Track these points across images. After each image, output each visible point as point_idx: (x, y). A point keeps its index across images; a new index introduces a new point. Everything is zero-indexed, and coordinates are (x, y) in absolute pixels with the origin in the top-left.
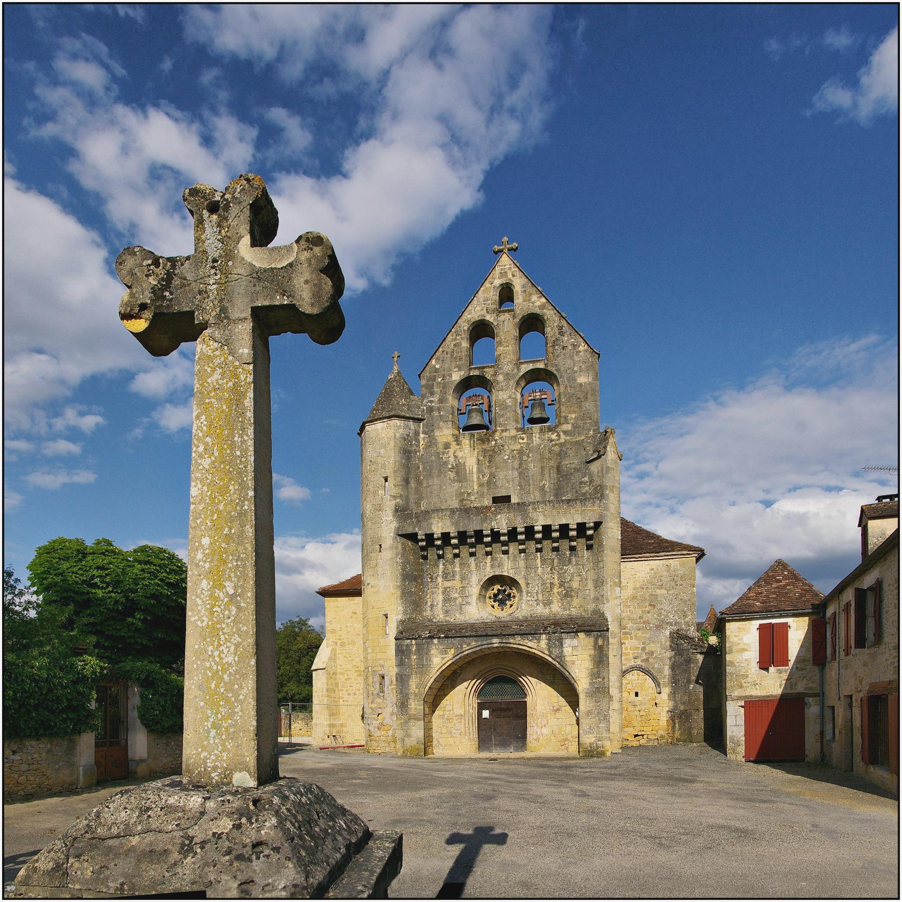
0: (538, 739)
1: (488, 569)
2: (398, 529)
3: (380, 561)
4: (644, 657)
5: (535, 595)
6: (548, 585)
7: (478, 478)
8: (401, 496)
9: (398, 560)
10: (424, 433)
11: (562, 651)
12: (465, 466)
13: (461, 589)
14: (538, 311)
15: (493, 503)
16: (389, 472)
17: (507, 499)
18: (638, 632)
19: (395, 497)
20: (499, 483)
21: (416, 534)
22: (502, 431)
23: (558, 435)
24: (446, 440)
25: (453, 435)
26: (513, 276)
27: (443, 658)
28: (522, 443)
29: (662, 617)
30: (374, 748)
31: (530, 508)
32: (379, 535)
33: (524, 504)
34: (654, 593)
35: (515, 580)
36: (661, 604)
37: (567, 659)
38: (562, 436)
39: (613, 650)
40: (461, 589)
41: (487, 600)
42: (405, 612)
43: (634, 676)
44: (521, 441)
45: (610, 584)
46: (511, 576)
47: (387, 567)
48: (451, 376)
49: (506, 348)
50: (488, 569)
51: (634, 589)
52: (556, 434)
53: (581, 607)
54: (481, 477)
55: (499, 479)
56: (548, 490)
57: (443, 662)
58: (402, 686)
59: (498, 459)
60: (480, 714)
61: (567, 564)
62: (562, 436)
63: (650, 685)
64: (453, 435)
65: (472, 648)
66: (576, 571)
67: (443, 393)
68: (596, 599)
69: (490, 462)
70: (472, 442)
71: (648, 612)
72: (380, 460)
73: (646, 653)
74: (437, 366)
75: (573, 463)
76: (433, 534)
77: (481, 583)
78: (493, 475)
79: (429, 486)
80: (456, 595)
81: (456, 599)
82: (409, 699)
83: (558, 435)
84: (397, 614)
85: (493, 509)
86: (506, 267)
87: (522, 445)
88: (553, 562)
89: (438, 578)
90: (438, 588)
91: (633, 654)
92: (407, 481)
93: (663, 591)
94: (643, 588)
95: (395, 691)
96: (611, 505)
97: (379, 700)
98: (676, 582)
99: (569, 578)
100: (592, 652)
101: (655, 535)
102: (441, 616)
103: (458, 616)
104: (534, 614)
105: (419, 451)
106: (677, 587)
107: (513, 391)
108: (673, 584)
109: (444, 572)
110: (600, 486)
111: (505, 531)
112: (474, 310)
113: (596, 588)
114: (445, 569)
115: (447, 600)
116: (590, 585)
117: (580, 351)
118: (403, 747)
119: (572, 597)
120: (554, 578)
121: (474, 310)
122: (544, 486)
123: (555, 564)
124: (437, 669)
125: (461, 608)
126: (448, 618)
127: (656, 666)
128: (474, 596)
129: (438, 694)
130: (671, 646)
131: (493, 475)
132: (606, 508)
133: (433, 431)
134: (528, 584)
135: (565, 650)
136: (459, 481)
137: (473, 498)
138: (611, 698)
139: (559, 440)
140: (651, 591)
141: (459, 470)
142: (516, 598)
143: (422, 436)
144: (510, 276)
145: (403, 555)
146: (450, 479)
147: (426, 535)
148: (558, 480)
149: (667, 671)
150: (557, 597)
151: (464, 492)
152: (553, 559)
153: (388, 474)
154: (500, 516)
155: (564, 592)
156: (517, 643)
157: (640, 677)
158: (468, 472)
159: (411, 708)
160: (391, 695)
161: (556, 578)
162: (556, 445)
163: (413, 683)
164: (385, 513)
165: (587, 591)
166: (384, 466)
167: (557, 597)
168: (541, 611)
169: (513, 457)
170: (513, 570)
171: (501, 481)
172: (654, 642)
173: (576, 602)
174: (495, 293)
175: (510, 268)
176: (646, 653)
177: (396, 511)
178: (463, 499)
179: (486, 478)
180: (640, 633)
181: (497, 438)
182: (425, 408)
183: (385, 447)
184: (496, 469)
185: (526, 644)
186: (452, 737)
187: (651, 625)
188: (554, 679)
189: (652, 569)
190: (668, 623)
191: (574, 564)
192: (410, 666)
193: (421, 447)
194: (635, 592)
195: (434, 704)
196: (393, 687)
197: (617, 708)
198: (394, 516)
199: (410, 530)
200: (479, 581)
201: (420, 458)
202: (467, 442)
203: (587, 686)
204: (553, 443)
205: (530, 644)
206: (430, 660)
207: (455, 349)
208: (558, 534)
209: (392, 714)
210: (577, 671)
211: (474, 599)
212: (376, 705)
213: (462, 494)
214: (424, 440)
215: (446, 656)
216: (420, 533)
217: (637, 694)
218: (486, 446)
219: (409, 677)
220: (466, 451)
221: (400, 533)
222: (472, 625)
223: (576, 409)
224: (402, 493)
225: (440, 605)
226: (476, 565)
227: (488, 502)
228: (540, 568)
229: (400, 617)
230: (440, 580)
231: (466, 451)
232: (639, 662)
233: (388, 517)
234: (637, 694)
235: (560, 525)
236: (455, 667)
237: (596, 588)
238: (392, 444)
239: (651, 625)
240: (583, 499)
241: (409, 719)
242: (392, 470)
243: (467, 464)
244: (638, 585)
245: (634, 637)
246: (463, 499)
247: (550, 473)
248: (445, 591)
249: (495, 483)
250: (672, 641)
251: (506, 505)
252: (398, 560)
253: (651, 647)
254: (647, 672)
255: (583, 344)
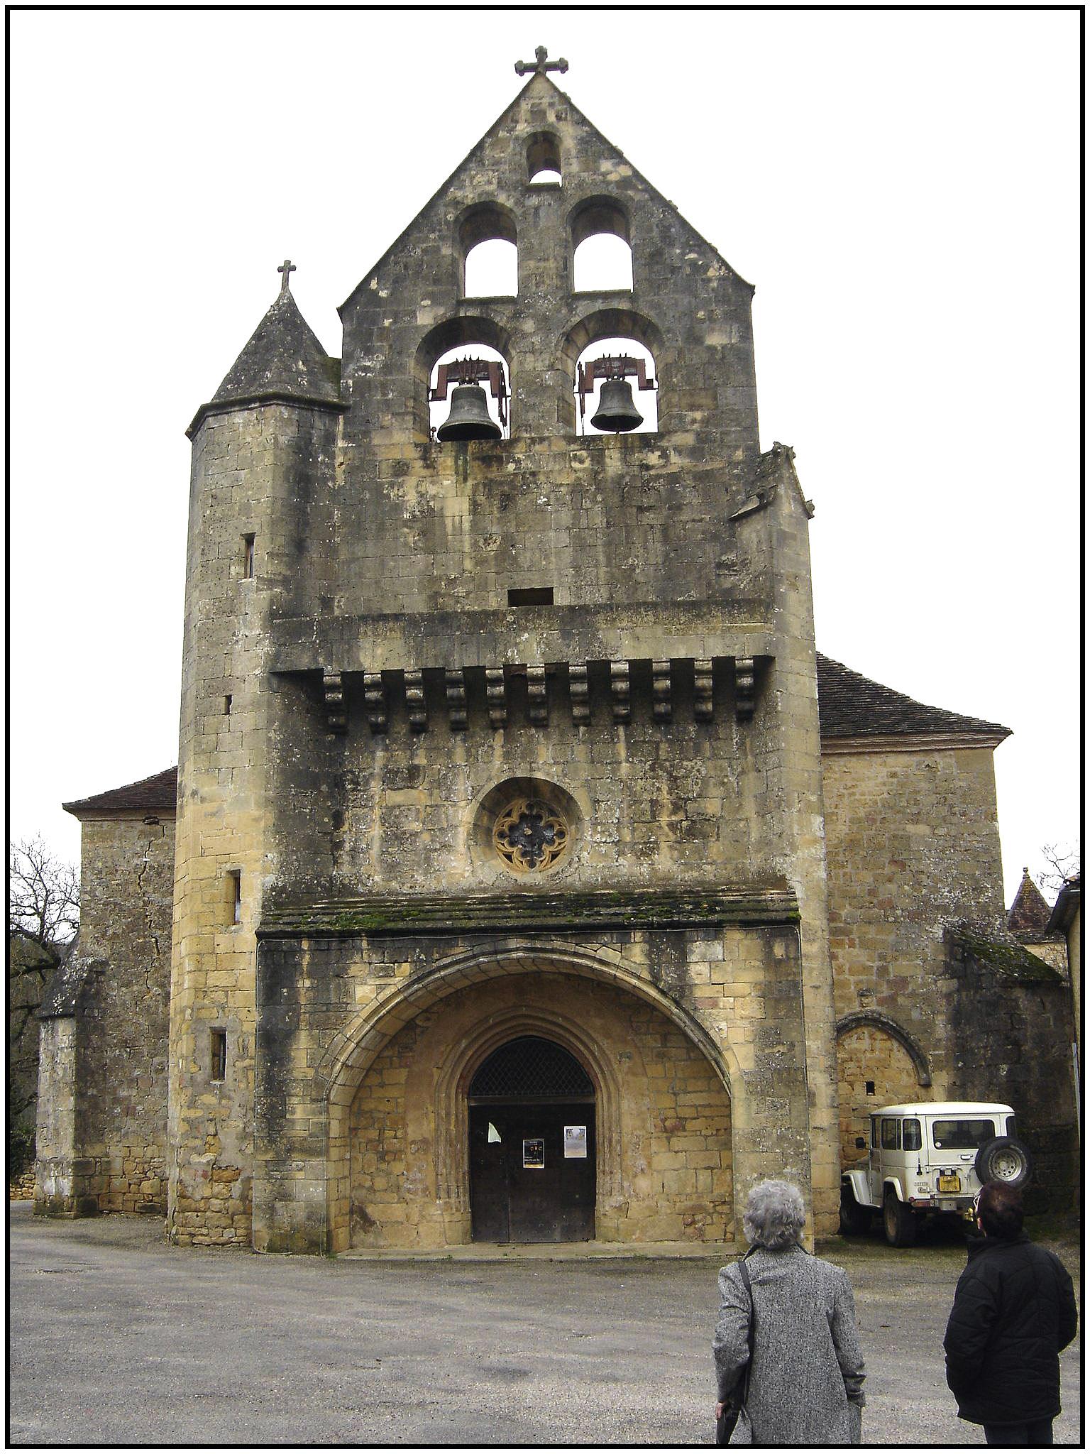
0: (623, 1209)
1: (497, 762)
2: (276, 657)
3: (226, 737)
4: (885, 991)
5: (613, 829)
6: (646, 806)
7: (475, 545)
8: (285, 582)
9: (272, 734)
10: (347, 437)
11: (686, 972)
12: (442, 516)
13: (429, 810)
14: (615, 192)
15: (511, 603)
16: (258, 524)
17: (543, 597)
18: (865, 928)
19: (271, 583)
20: (525, 559)
21: (319, 673)
22: (533, 441)
23: (664, 456)
24: (399, 457)
25: (416, 445)
26: (559, 118)
27: (381, 988)
28: (580, 470)
29: (924, 891)
30: (192, 1230)
31: (600, 618)
32: (227, 673)
33: (584, 609)
34: (901, 833)
35: (563, 792)
36: (919, 860)
37: (698, 993)
38: (674, 458)
39: (810, 973)
40: (429, 810)
41: (495, 840)
42: (284, 867)
43: (860, 1042)
44: (576, 465)
45: (797, 806)
46: (555, 780)
47: (243, 753)
48: (413, 315)
49: (542, 264)
50: (497, 762)
51: (852, 821)
52: (659, 453)
53: (728, 860)
54: (481, 544)
55: (525, 548)
56: (641, 579)
57: (382, 997)
58: (273, 1062)
59: (522, 502)
60: (477, 1136)
61: (690, 757)
62: (674, 458)
63: (902, 1065)
64: (416, 445)
65: (457, 962)
66: (712, 773)
67: (398, 351)
68: (765, 843)
69: (504, 508)
70: (460, 463)
71: (890, 880)
72: (237, 495)
73: (888, 982)
74: (383, 294)
75: (701, 520)
76: (362, 674)
77: (480, 797)
78: (509, 541)
79: (354, 560)
80: (416, 826)
81: (415, 834)
82: (290, 1095)
83: (664, 456)
84: (265, 872)
85: (510, 618)
86: (544, 100)
87: (580, 474)
88: (657, 749)
89: (373, 784)
90: (372, 808)
91: (857, 983)
92: (298, 546)
93: (922, 829)
94: (874, 820)
95: (251, 1074)
96: (792, 619)
97: (209, 1099)
98: (951, 806)
99: (696, 789)
100: (760, 976)
101: (896, 693)
102: (377, 878)
103: (420, 878)
104: (612, 877)
105: (333, 478)
106: (955, 820)
107: (559, 354)
108: (944, 811)
109: (386, 766)
110: (766, 574)
111: (541, 671)
112: (471, 183)
113: (763, 816)
114: (388, 759)
115: (395, 836)
116: (750, 809)
117: (709, 280)
118: (270, 1227)
119: (705, 836)
120: (659, 789)
121: (471, 183)
122: (633, 568)
123: (663, 754)
124: (364, 1014)
125: (428, 859)
126: (394, 885)
127: (915, 1015)
128: (461, 829)
129: (368, 1082)
130: (947, 965)
131: (509, 541)
132: (782, 628)
133: (366, 434)
134: (598, 802)
135: (693, 969)
136: (430, 551)
137: (461, 591)
138: (811, 1098)
139: (664, 466)
140: (892, 826)
141: (429, 520)
142: (567, 838)
143: (341, 443)
144: (551, 118)
145: (283, 722)
146: (406, 544)
147: (344, 675)
148: (666, 555)
149: (942, 1028)
150: (667, 836)
151: (441, 578)
152: (658, 744)
153: (256, 529)
154: (526, 635)
155: (685, 824)
156: (564, 951)
157: (878, 1044)
158: (449, 529)
159: (293, 1122)
160: (243, 1086)
161: (665, 789)
162: (659, 477)
163: (302, 1049)
164: (245, 620)
165: (742, 824)
166: (246, 509)
167: (667, 836)
168: (630, 869)
169: (557, 500)
170: (560, 768)
171: (528, 554)
172: (905, 954)
173: (716, 849)
174: (518, 149)
175: (551, 105)
176: (888, 982)
177: (272, 615)
178: (437, 593)
179: (494, 547)
180: (871, 932)
181: (521, 456)
182: (350, 382)
183: (251, 467)
184: (517, 526)
185: (592, 953)
186: (403, 1200)
187: (899, 912)
188: (664, 1045)
189: (893, 775)
190: (937, 907)
191: (708, 754)
192: (293, 1002)
193: (339, 472)
194: (855, 828)
195: (355, 1109)
196: (247, 1062)
197: (825, 1124)
198: (263, 627)
199: (304, 662)
200: (475, 792)
201: (335, 494)
202: (450, 462)
203: (749, 1065)
204: (652, 472)
205: (603, 953)
206: (346, 993)
207: (425, 258)
208: (668, 682)
209: (244, 1136)
210: (723, 1025)
211: (461, 837)
212: (199, 1113)
213: (434, 580)
214: (345, 454)
215: (389, 981)
216: (328, 669)
217: (870, 1087)
218: (494, 474)
219: (290, 1034)
220: (446, 483)
221: (280, 667)
222: (458, 901)
223: (703, 401)
224: (288, 573)
225: (375, 851)
226: (468, 751)
227: (496, 601)
228: (624, 764)
229: (271, 879)
230: (375, 786)
231: (446, 483)
232: (872, 1005)
233: (251, 629)
234: (870, 1087)
235: (672, 661)
236: (410, 1013)
237: (763, 816)
238: (269, 459)
239: (899, 912)
240: (731, 603)
241: (288, 1151)
242: (265, 519)
243: (448, 513)
244: (862, 813)
245: (857, 941)
246: (437, 593)
247: (646, 541)
248: (391, 817)
249: (515, 558)
250: (951, 954)
251: (544, 609)
252: (272, 734)
253: (900, 967)
254: (896, 1033)
255: (717, 266)
